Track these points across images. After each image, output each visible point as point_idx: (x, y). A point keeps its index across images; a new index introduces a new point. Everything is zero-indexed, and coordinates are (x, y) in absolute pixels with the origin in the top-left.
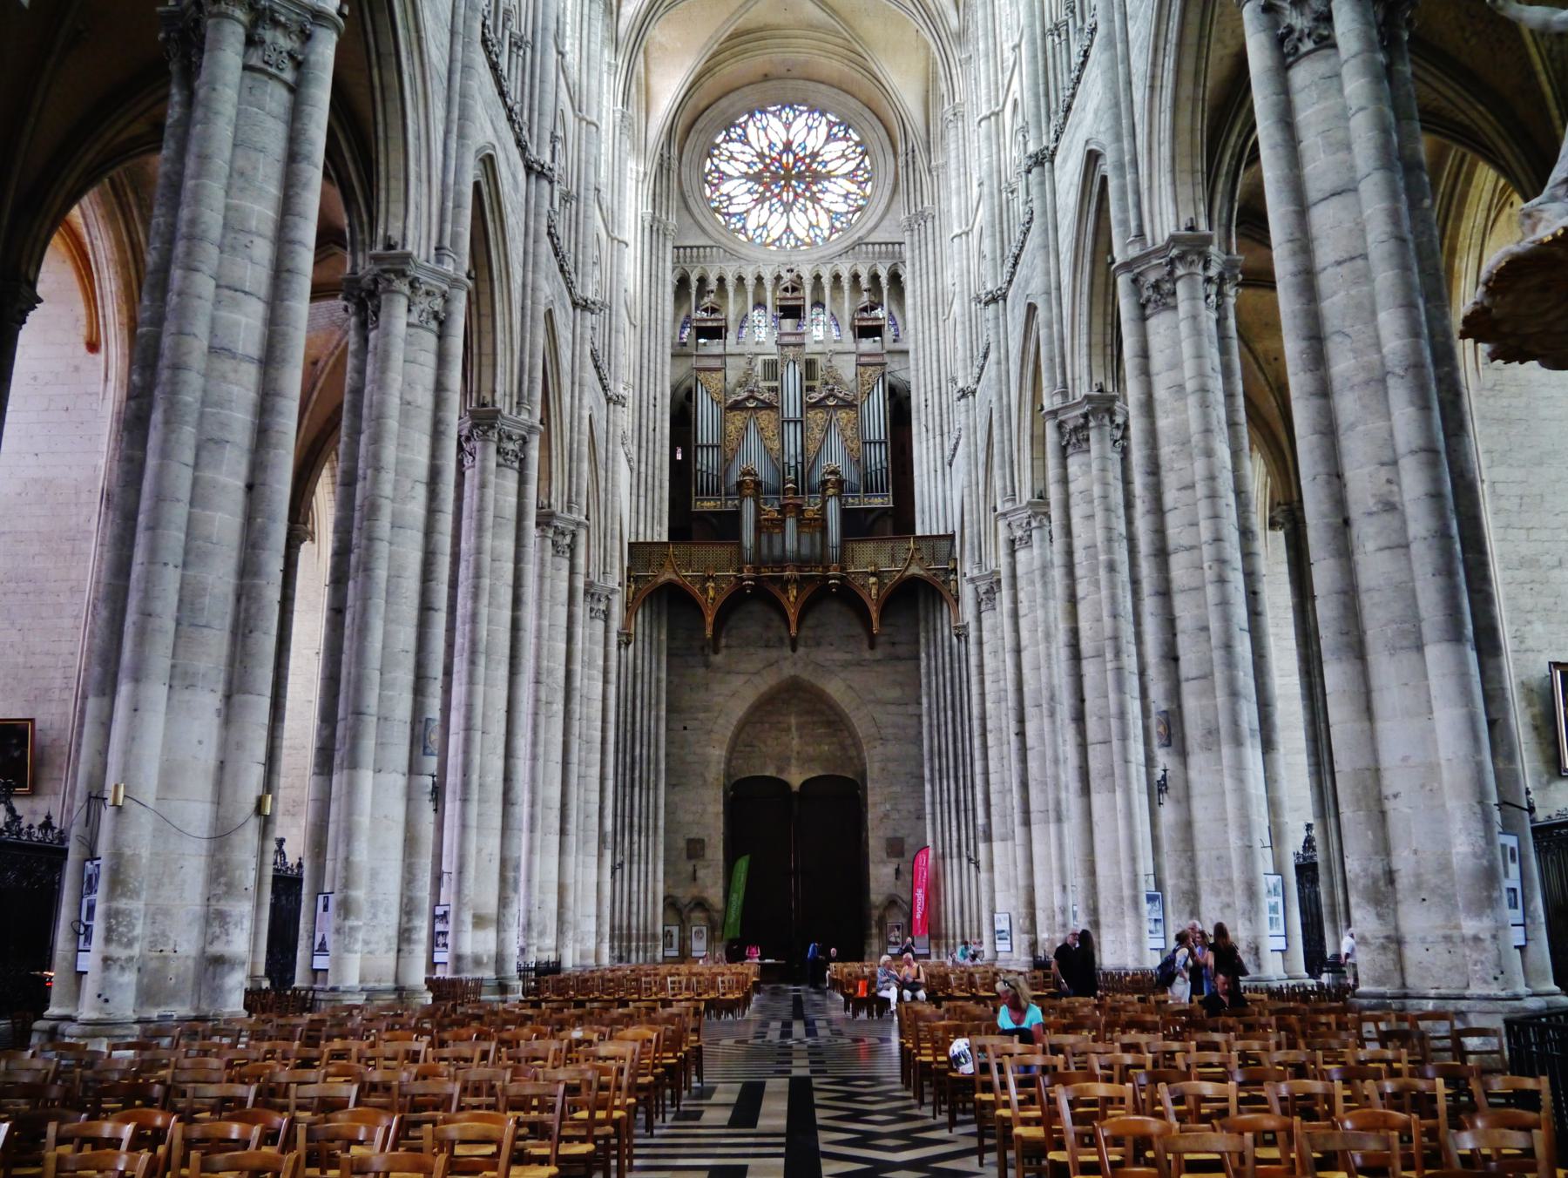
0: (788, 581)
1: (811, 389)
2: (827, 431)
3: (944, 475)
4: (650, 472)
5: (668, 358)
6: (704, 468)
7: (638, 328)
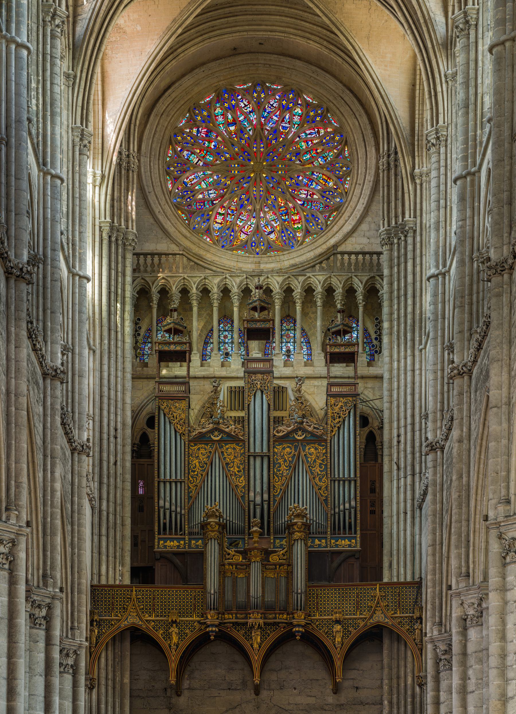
0: (252, 627)
1: (278, 421)
2: (294, 468)
3: (413, 517)
4: (111, 509)
5: (129, 384)
6: (167, 505)
7: (98, 352)
